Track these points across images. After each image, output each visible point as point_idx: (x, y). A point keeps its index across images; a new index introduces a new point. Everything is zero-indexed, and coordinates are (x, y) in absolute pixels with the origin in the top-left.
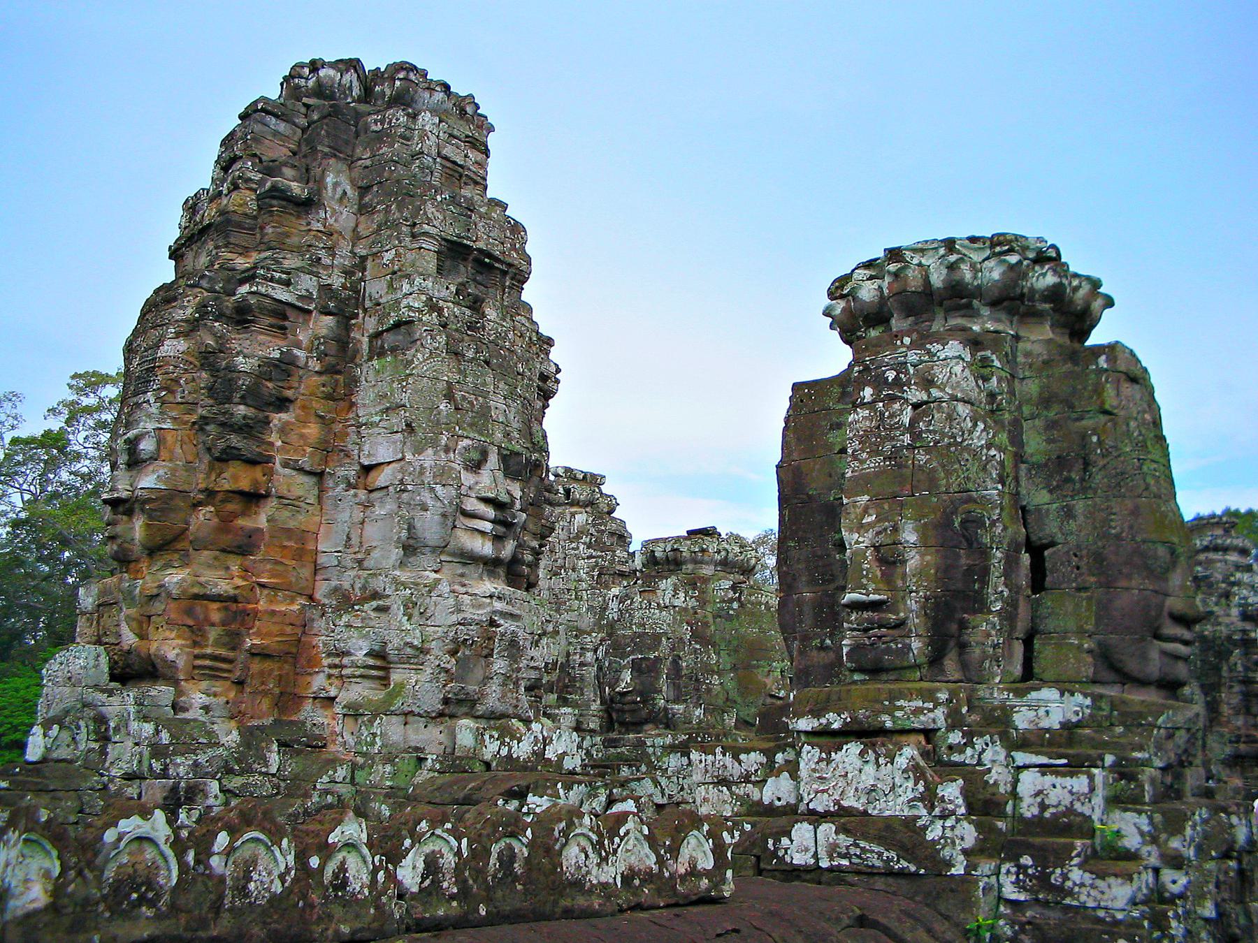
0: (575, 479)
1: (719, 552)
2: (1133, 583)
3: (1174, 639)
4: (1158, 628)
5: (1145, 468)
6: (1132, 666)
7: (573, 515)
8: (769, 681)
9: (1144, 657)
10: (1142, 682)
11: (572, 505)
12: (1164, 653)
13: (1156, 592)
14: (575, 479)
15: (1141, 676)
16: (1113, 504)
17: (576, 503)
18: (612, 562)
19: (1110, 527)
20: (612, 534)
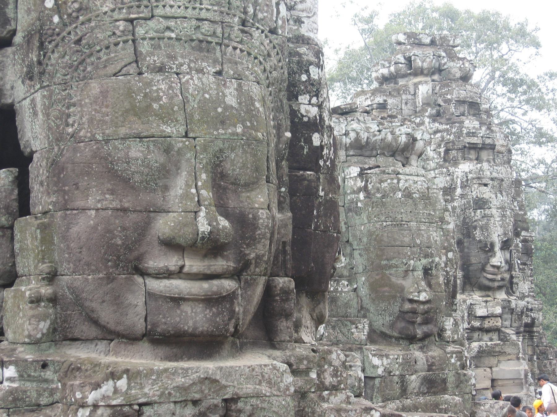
0: (420, 44)
1: (346, 134)
2: (91, 202)
3: (168, 274)
4: (140, 258)
5: (140, 31)
6: (106, 315)
7: (416, 85)
8: (407, 283)
9: (117, 301)
10: (130, 338)
11: (415, 74)
12: (150, 295)
13: (124, 210)
14: (420, 44)
15: (120, 328)
16: (72, 92)
17: (419, 72)
18: (459, 134)
19: (67, 125)
20: (461, 102)
